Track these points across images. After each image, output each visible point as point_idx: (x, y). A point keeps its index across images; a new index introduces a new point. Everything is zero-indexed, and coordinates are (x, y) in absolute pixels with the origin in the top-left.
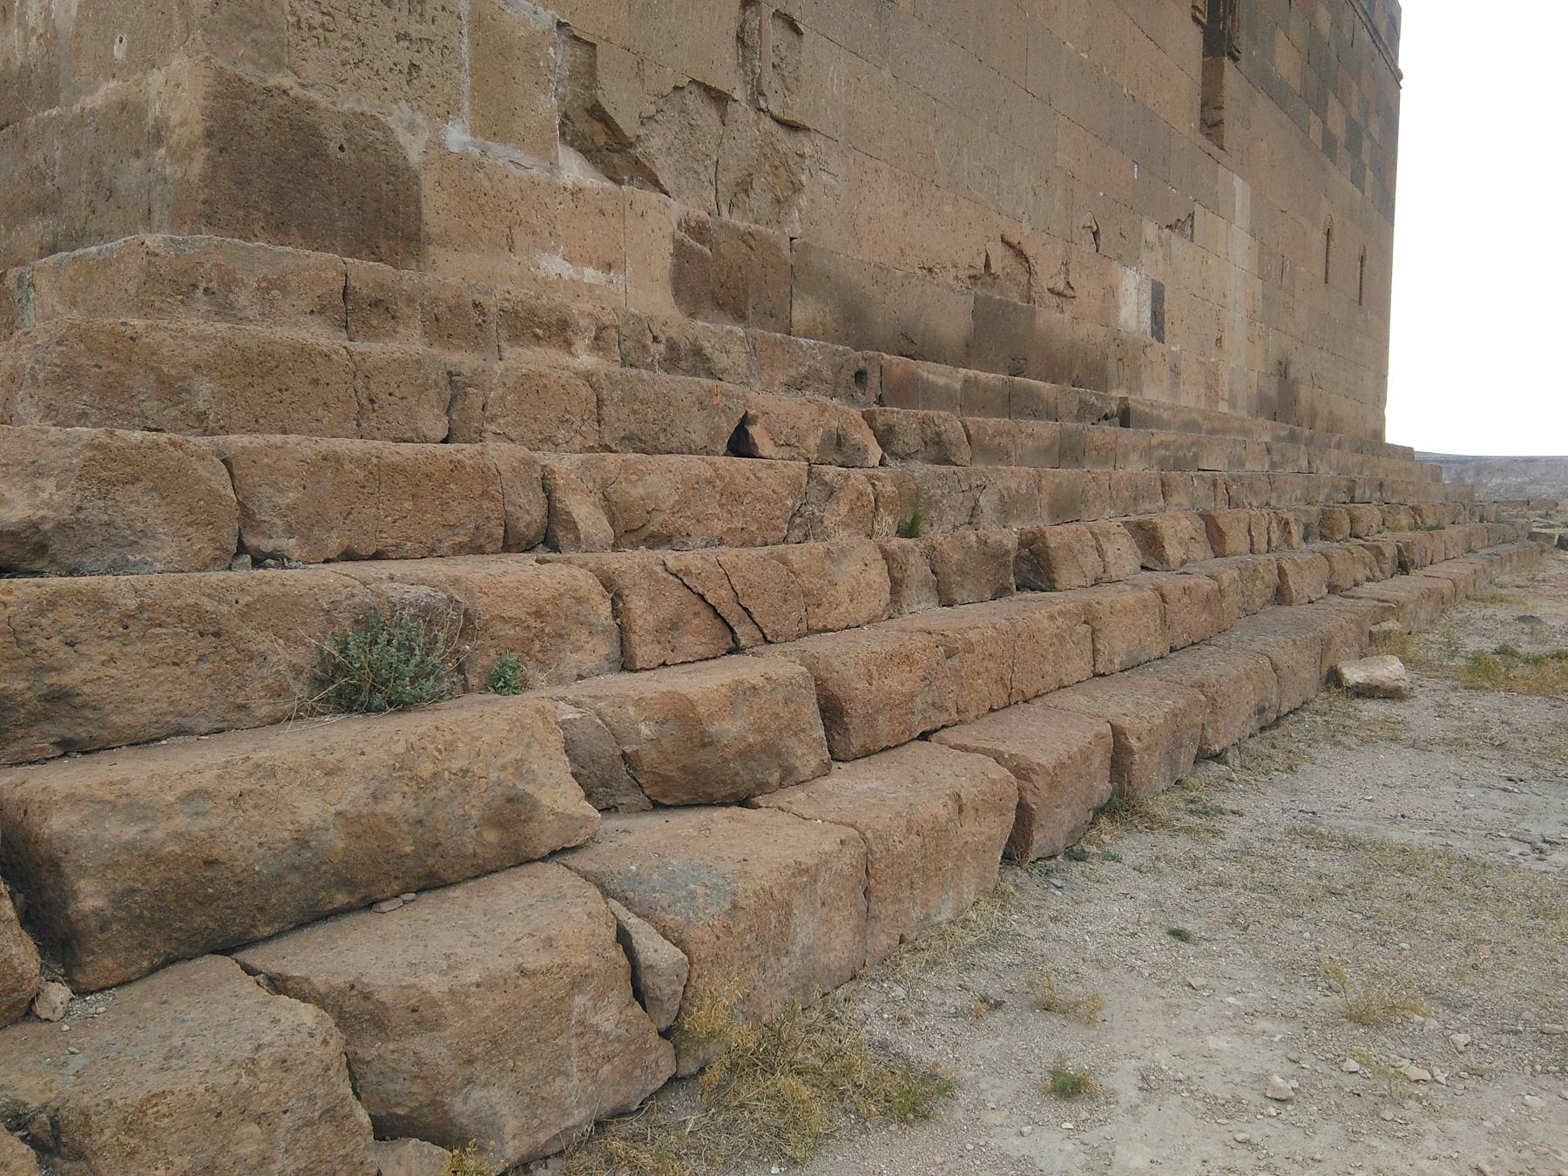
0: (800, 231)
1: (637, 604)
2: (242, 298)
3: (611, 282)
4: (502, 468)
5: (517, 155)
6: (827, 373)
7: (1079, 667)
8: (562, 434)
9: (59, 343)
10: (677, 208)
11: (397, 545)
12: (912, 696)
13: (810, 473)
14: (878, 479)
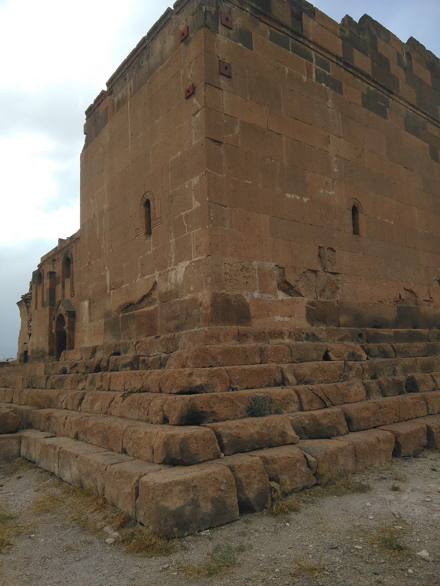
0: (340, 299)
1: (303, 397)
2: (221, 338)
3: (291, 320)
4: (273, 369)
5: (269, 296)
6: (350, 336)
7: (423, 412)
8: (284, 359)
9: (195, 351)
10: (306, 299)
11: (255, 386)
12: (370, 417)
13: (345, 363)
14: (363, 364)
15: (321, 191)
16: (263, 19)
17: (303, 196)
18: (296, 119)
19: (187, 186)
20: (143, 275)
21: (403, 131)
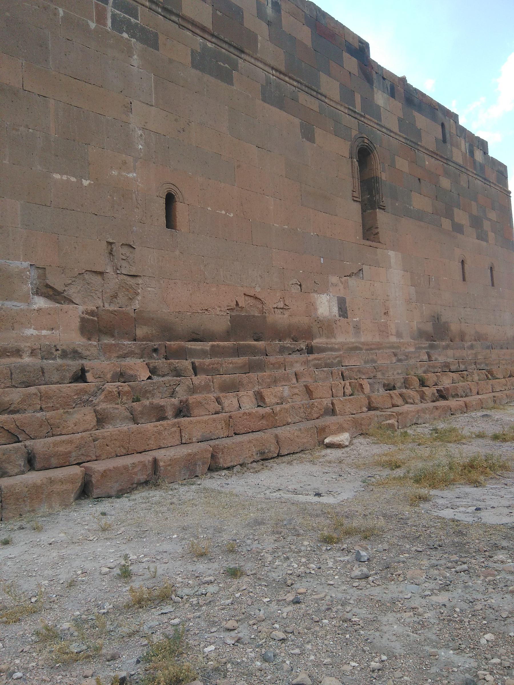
0: (138, 307)
5: (15, 303)
6: (137, 351)
10: (81, 308)
12: (70, 452)
15: (114, 173)
17: (82, 177)
18: (75, 79)
21: (259, 102)
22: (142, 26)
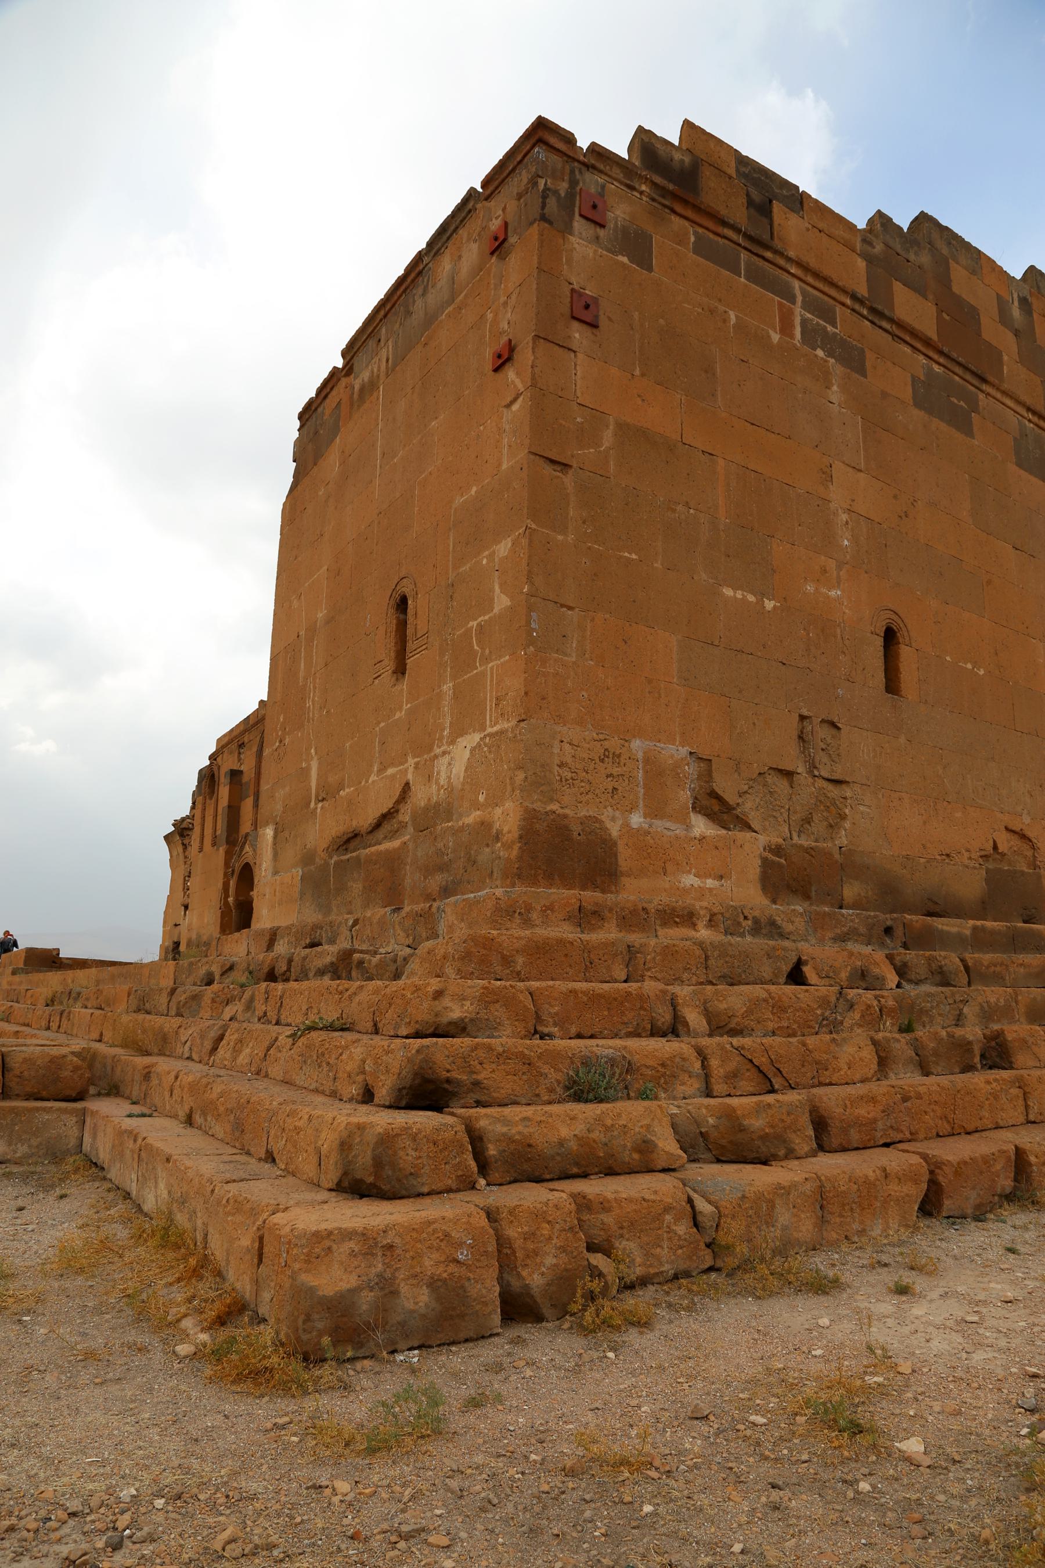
0: (846, 842)
1: (714, 1062)
2: (534, 916)
3: (723, 885)
4: (650, 994)
5: (668, 824)
6: (862, 930)
7: (1017, 1115)
8: (686, 976)
9: (464, 943)
10: (762, 839)
11: (601, 1032)
12: (875, 1121)
13: (840, 993)
14: (883, 997)
15: (810, 588)
16: (678, 208)
17: (763, 595)
18: (753, 424)
19: (485, 562)
20: (382, 769)
21: (1012, 467)
22: (842, 338)
